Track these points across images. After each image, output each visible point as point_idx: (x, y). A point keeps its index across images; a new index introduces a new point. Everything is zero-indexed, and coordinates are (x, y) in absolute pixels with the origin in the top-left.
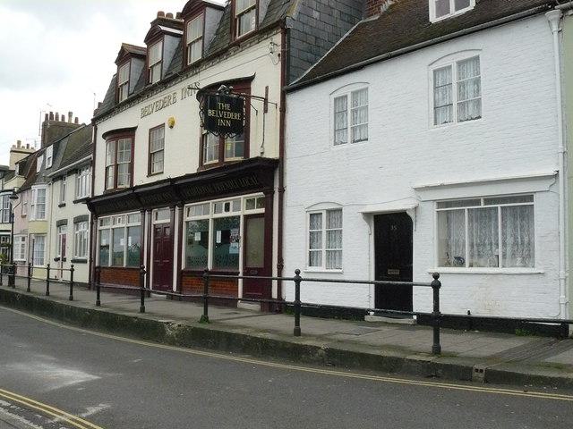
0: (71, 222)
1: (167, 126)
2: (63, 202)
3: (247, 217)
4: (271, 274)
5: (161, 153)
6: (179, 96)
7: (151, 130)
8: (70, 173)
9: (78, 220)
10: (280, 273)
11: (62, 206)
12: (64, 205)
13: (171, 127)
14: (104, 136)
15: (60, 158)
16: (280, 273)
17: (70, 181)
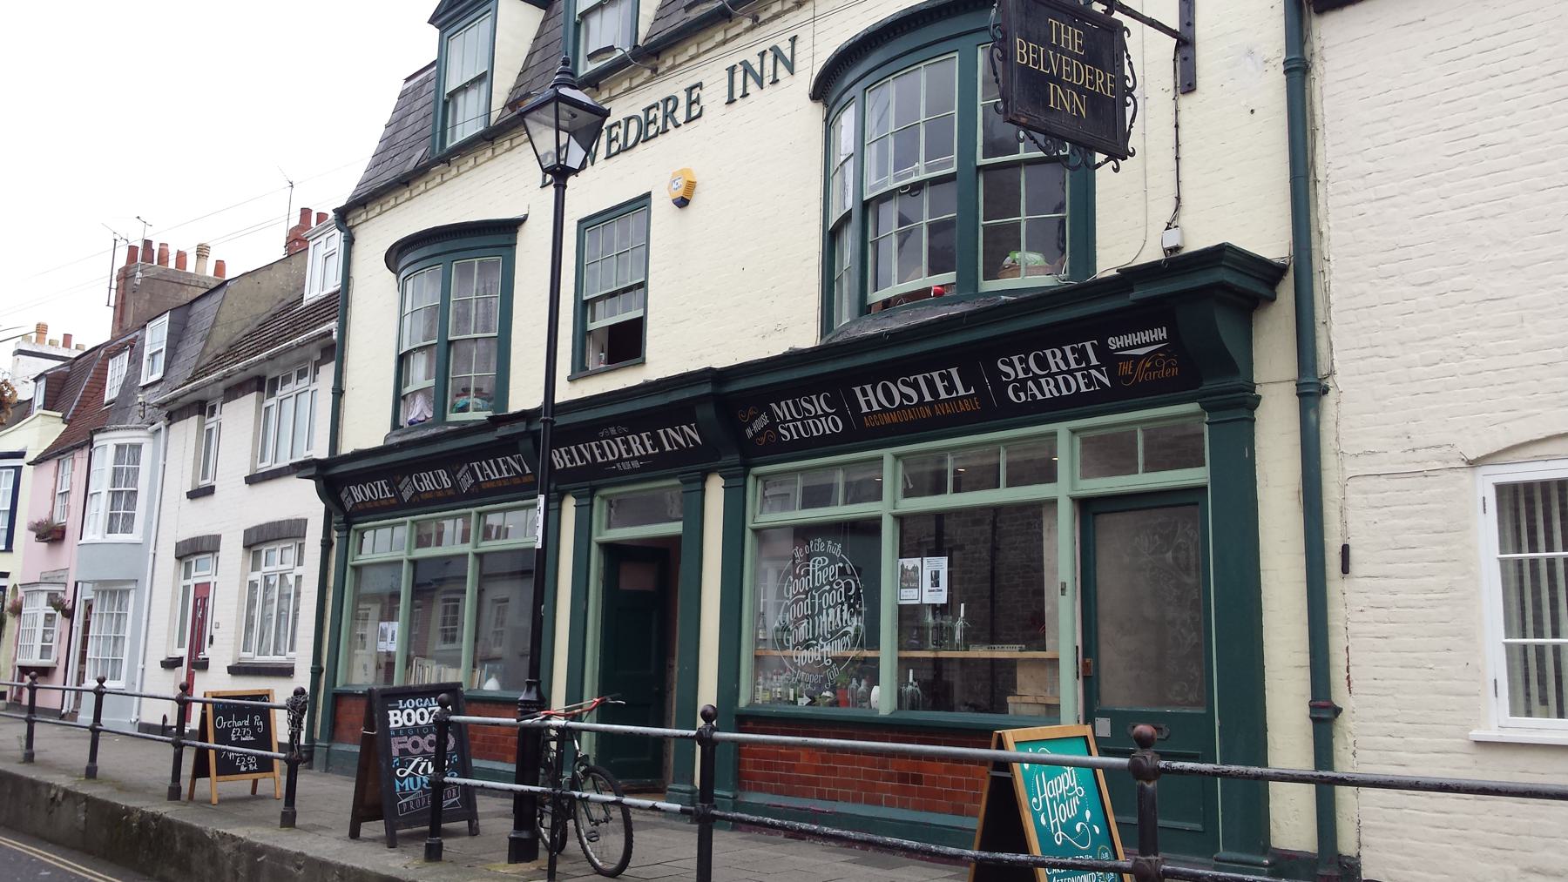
0: (232, 548)
1: (661, 207)
2: (206, 483)
3: (1087, 507)
4: (1257, 748)
5: (641, 291)
6: (712, 97)
7: (580, 222)
8: (234, 391)
9: (258, 540)
10: (1323, 749)
11: (201, 493)
12: (209, 491)
13: (682, 203)
14: (397, 255)
15: (192, 350)
16: (1323, 749)
17: (238, 417)
